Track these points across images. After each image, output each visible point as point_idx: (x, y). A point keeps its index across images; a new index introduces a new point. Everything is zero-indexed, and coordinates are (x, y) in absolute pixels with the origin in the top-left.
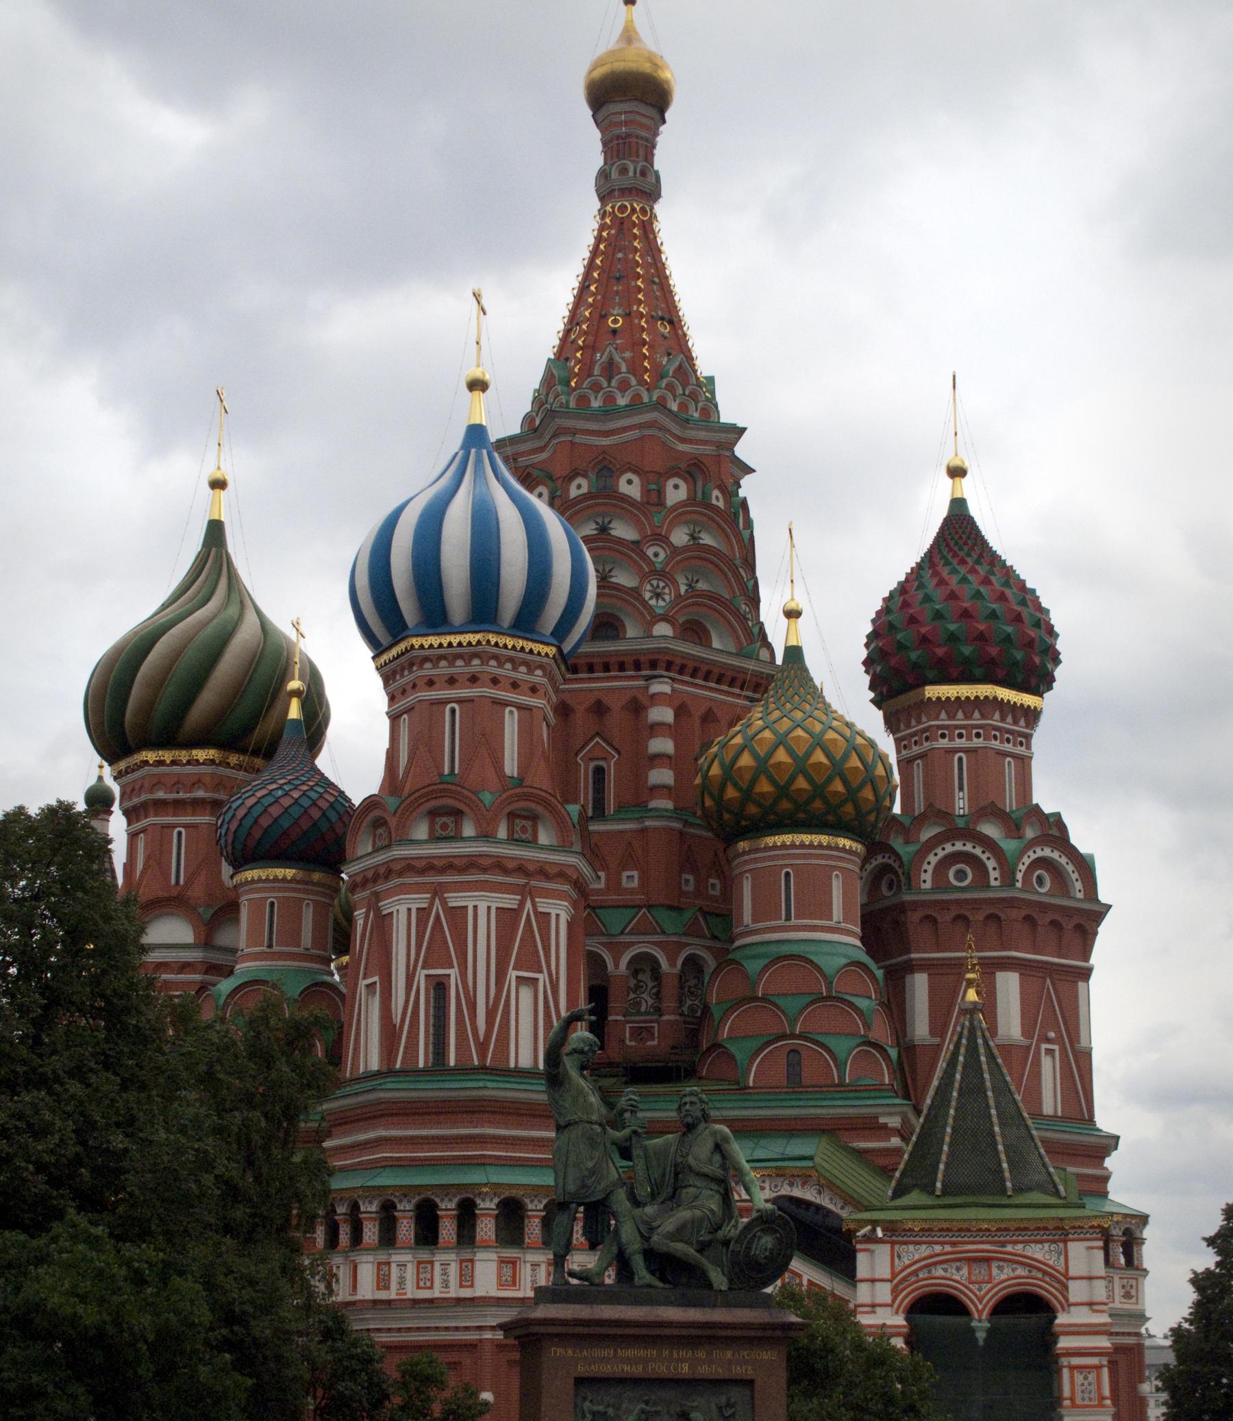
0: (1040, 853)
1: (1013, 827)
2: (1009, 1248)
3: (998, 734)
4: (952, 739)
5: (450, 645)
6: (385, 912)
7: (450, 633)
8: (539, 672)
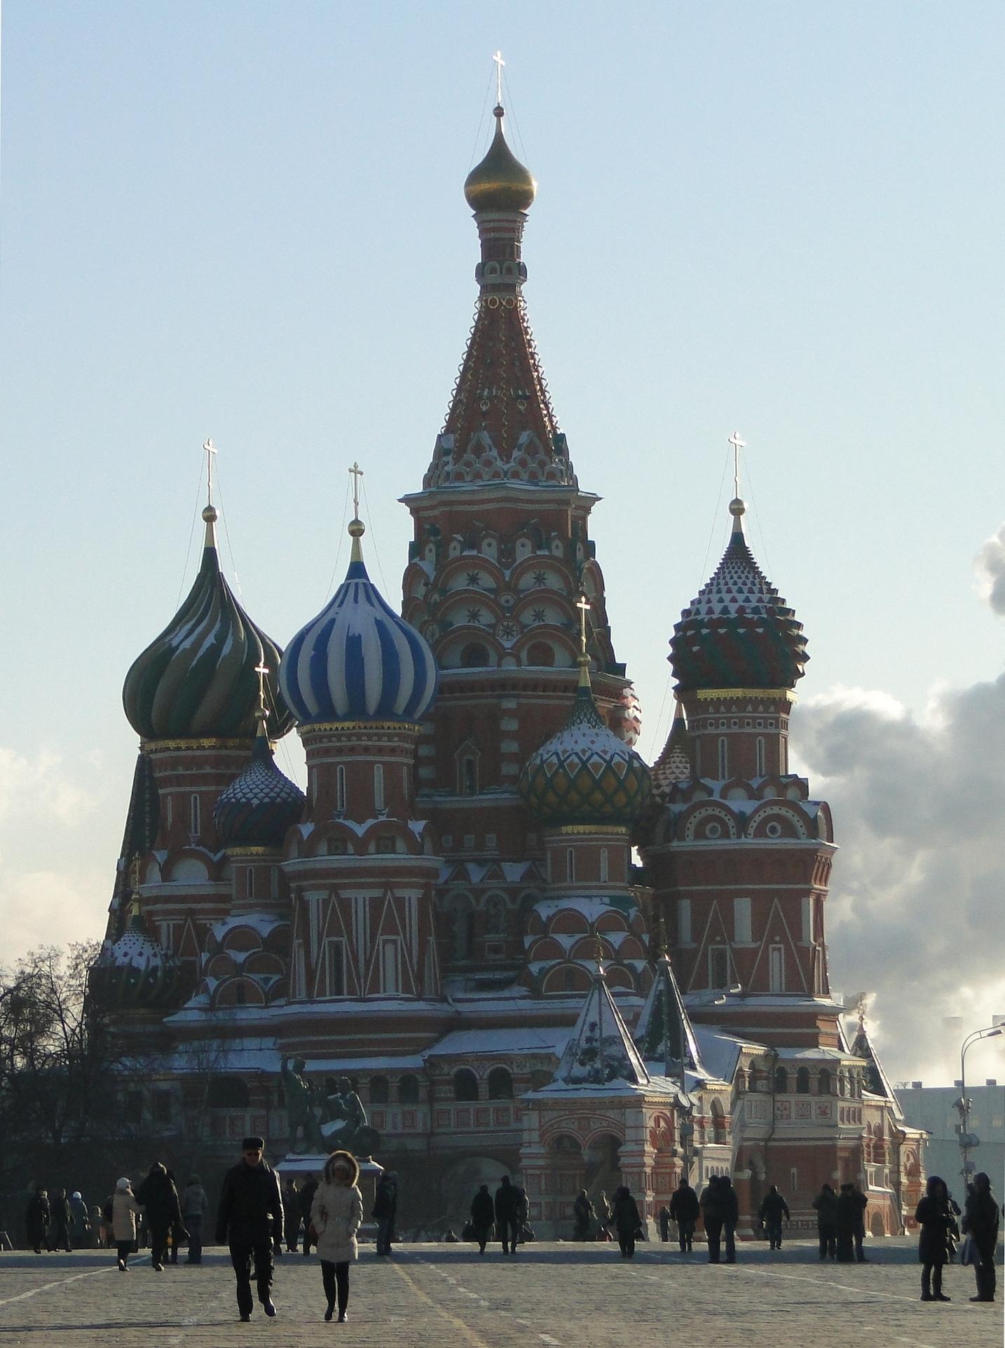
0: (769, 811)
1: (754, 795)
2: (597, 1112)
3: (750, 721)
4: (717, 727)
5: (337, 729)
6: (306, 898)
7: (337, 721)
8: (396, 739)
